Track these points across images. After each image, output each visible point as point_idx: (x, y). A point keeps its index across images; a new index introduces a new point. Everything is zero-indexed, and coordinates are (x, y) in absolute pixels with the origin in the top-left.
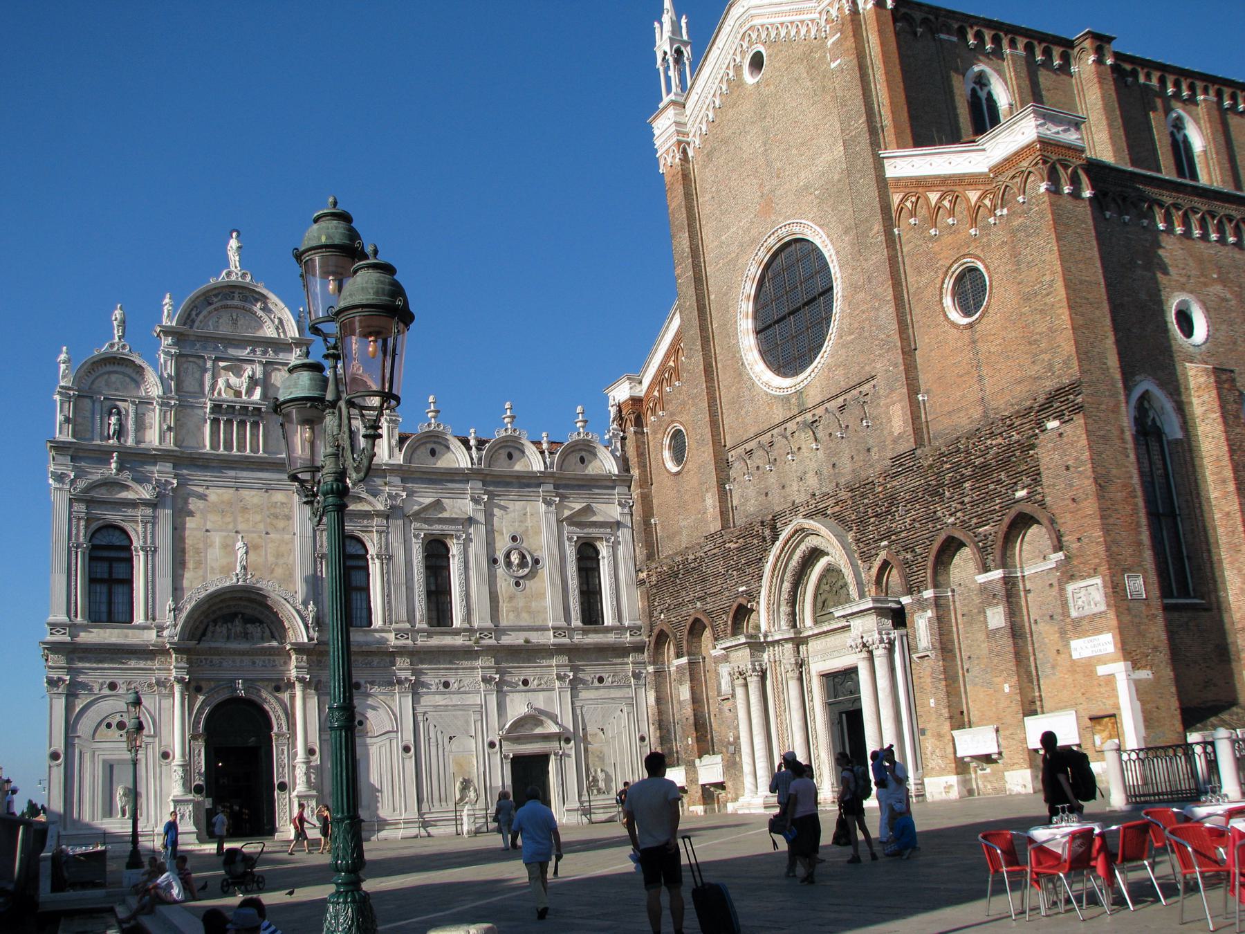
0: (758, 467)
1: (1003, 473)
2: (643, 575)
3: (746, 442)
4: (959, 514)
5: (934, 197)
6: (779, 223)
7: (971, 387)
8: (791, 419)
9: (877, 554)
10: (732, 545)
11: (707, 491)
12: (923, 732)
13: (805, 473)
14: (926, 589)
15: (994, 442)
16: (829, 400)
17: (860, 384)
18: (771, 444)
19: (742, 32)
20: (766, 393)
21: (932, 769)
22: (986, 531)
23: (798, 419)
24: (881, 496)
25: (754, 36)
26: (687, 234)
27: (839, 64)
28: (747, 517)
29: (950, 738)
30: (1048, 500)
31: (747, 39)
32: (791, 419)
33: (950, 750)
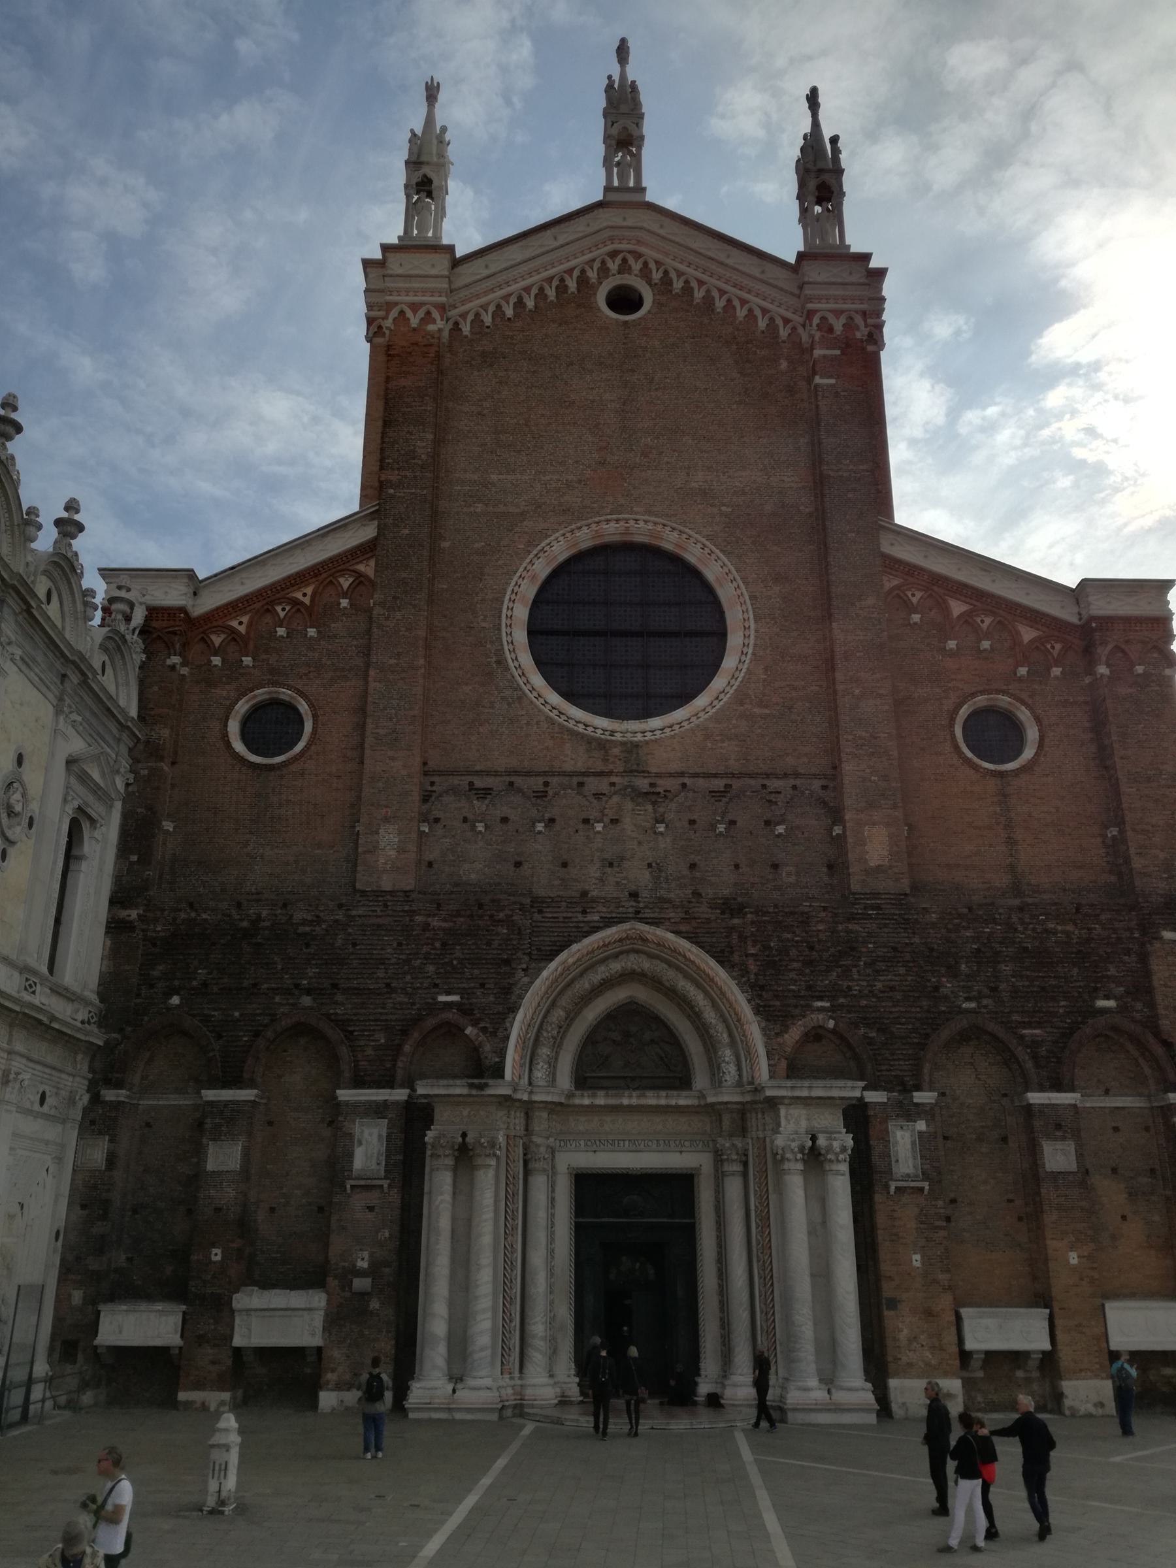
0: (505, 820)
1: (1076, 970)
2: (134, 914)
3: (478, 773)
4: (985, 1002)
5: (958, 608)
6: (632, 512)
7: (991, 846)
8: (601, 774)
9: (804, 1017)
10: (435, 922)
11: (386, 820)
12: (893, 1304)
13: (622, 858)
14: (918, 1088)
15: (1059, 928)
16: (696, 775)
17: (768, 776)
18: (541, 795)
19: (610, 247)
20: (552, 722)
21: (910, 1365)
22: (1032, 1035)
23: (614, 779)
24: (822, 937)
25: (636, 266)
26: (430, 437)
27: (832, 385)
28: (457, 885)
29: (954, 1318)
30: (1165, 1024)
31: (618, 260)
32: (601, 774)
33: (950, 1337)
